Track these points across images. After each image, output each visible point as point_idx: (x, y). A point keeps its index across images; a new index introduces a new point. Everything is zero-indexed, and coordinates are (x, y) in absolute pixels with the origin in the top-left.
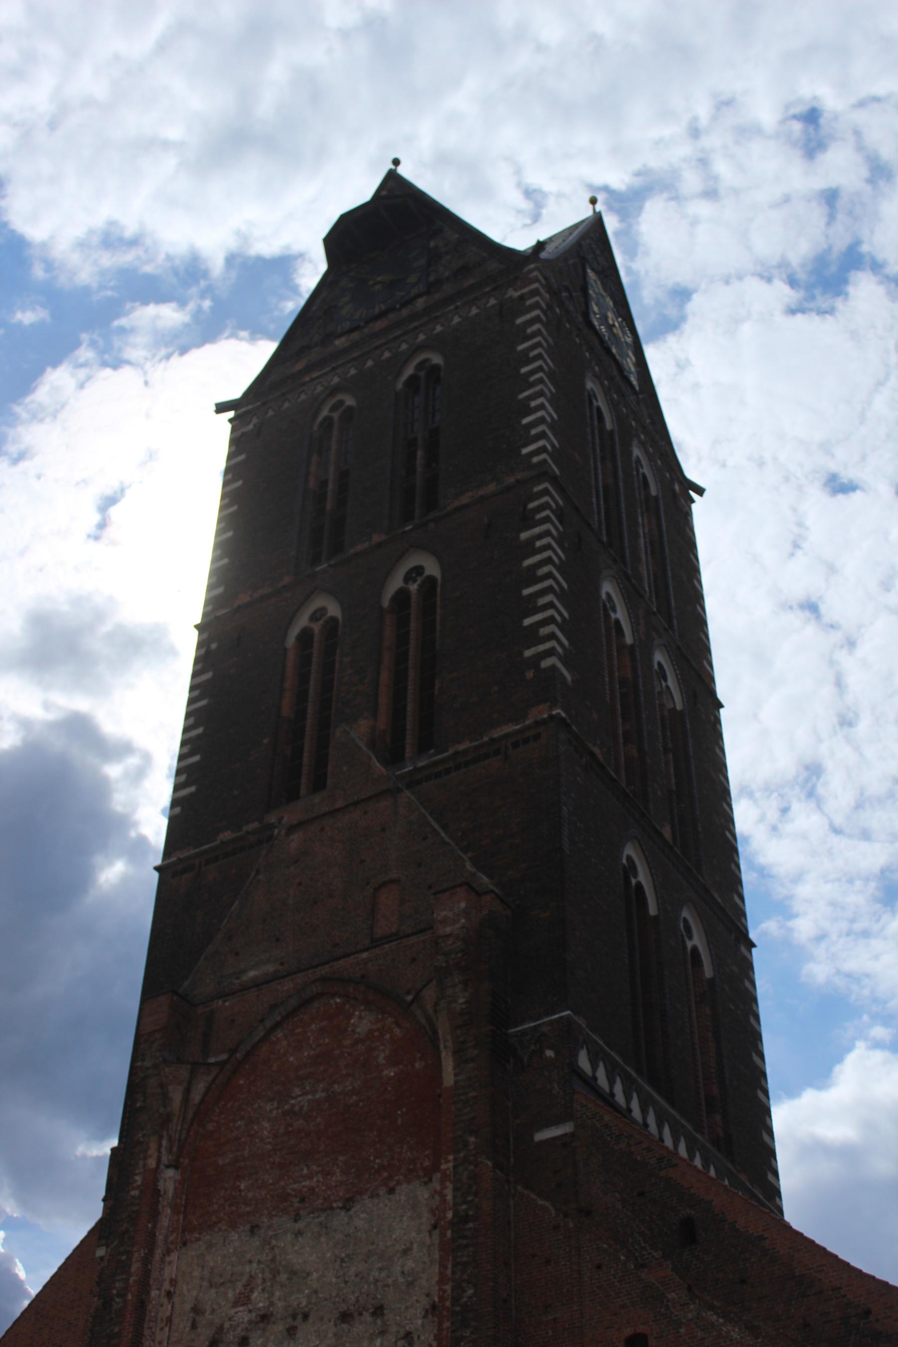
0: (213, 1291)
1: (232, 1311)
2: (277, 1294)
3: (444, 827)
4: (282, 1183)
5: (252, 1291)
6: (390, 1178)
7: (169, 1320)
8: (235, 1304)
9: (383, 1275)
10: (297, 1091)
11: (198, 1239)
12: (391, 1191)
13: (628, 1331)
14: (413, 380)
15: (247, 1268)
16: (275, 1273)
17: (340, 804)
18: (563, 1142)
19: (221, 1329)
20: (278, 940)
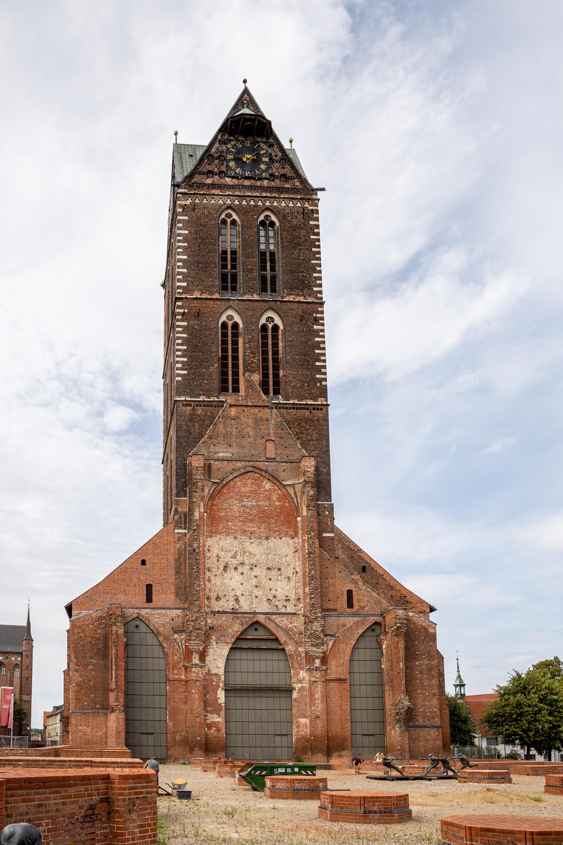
0: (223, 552)
1: (231, 559)
2: (246, 558)
3: (290, 428)
4: (244, 527)
5: (237, 555)
6: (280, 534)
7: (209, 557)
8: (232, 558)
9: (280, 560)
10: (246, 500)
11: (216, 536)
12: (281, 538)
13: (348, 589)
14: (263, 223)
15: (235, 549)
16: (245, 552)
17: (249, 404)
18: (332, 539)
19: (228, 563)
20: (230, 446)
